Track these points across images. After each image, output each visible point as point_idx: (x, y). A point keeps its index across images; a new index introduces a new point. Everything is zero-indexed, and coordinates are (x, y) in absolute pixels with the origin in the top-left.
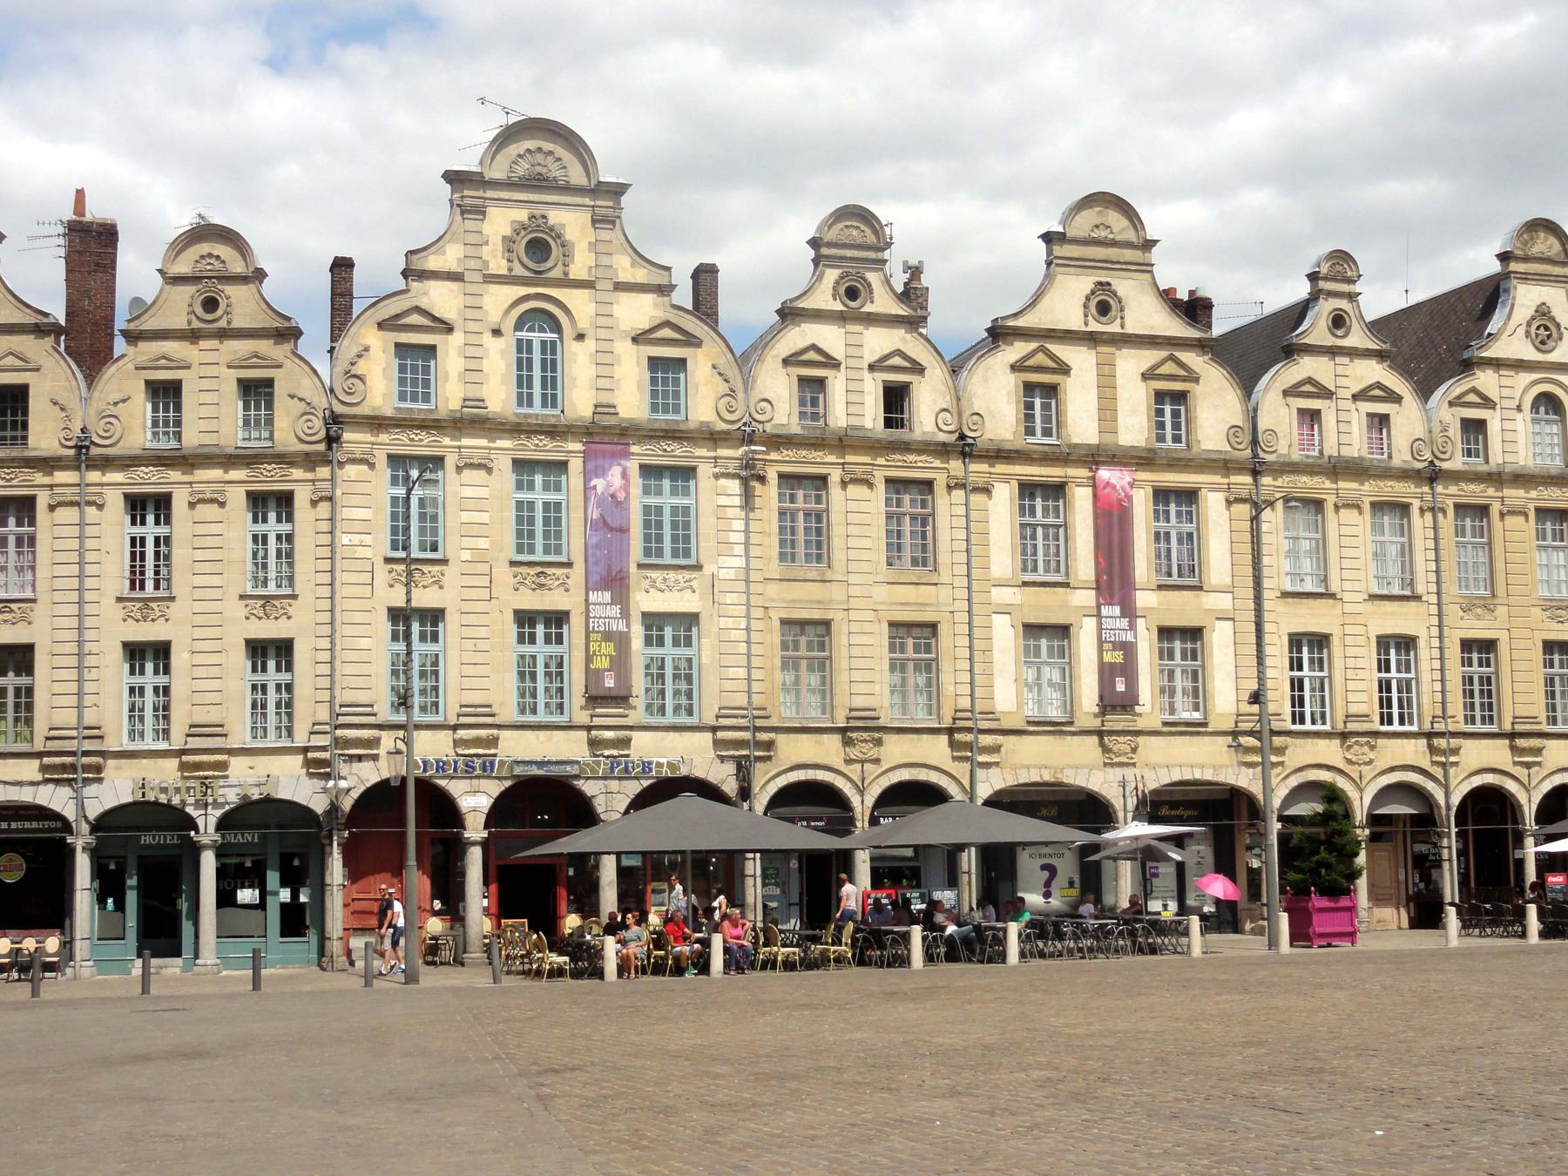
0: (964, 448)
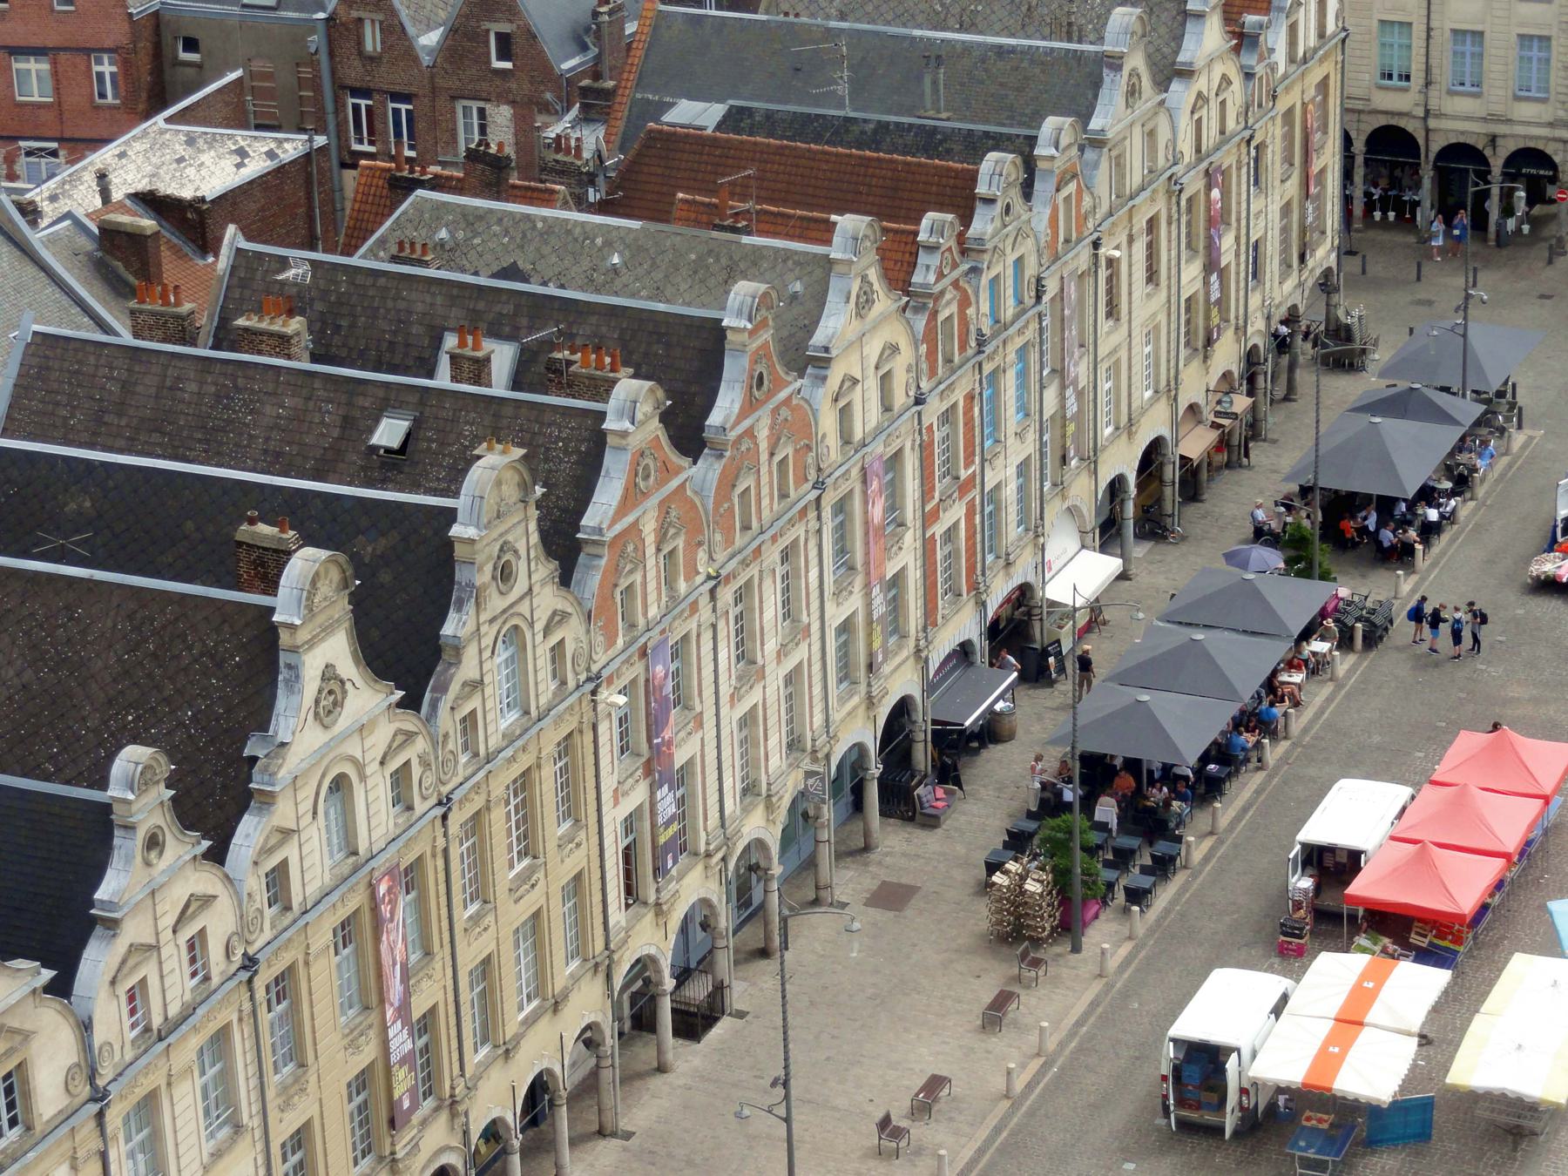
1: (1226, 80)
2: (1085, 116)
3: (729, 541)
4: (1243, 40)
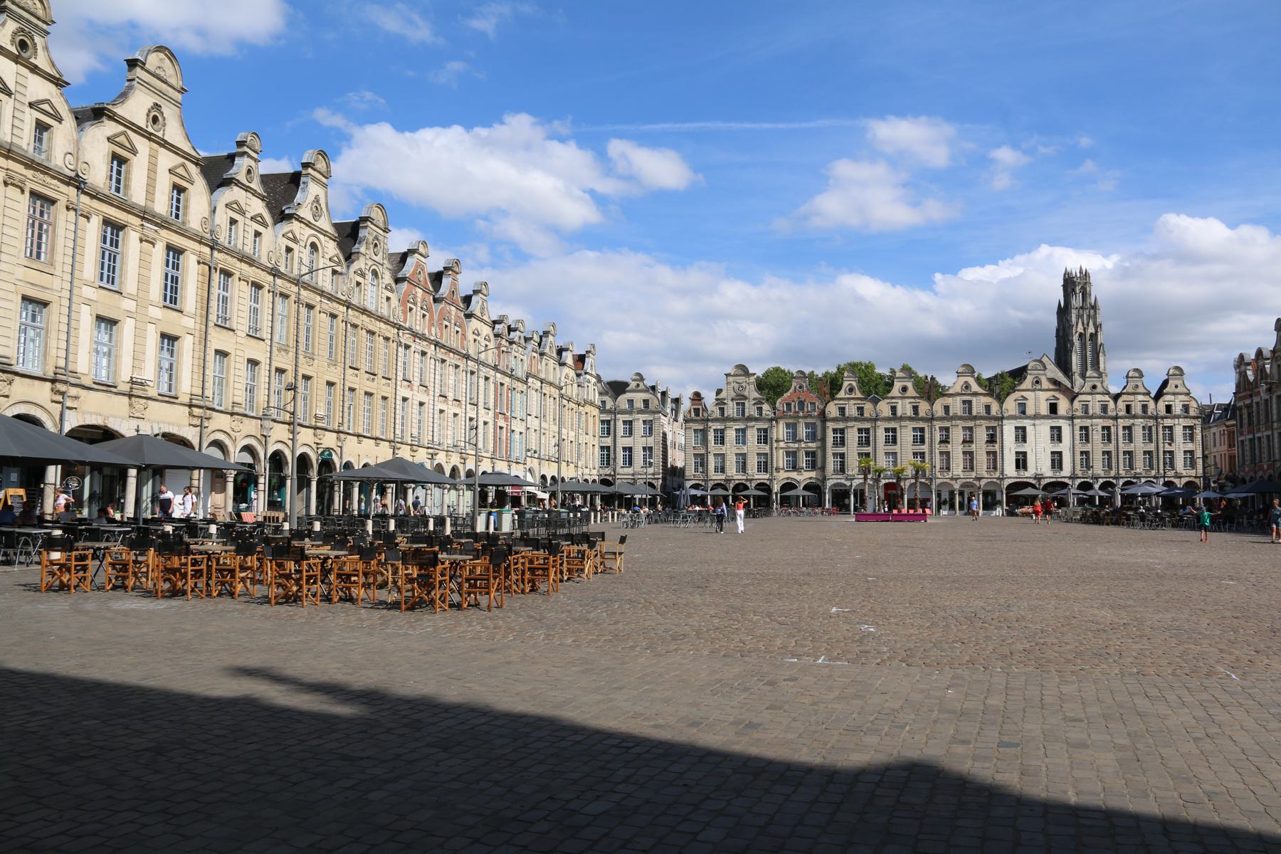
0: (77, 182)
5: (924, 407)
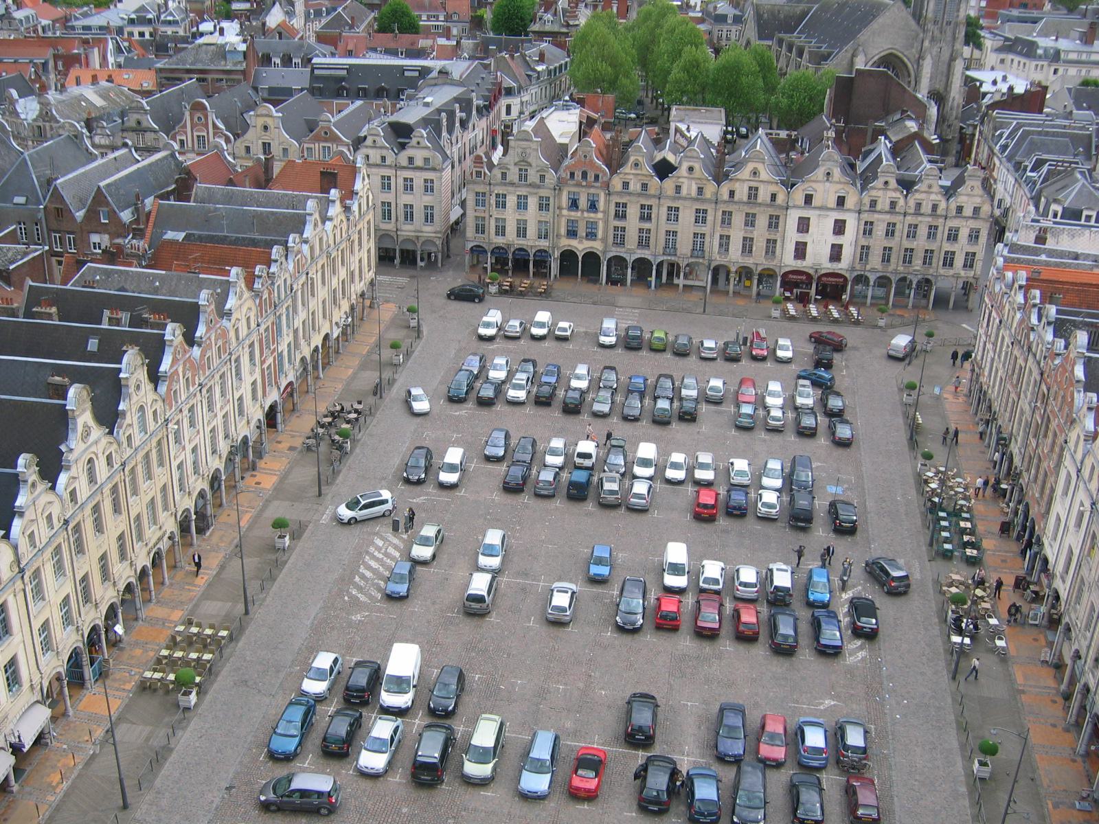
1: (341, 220)
2: (302, 234)
3: (204, 374)
4: (347, 209)
5: (710, 188)
